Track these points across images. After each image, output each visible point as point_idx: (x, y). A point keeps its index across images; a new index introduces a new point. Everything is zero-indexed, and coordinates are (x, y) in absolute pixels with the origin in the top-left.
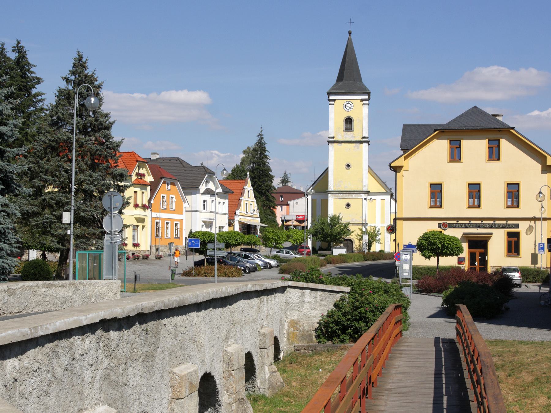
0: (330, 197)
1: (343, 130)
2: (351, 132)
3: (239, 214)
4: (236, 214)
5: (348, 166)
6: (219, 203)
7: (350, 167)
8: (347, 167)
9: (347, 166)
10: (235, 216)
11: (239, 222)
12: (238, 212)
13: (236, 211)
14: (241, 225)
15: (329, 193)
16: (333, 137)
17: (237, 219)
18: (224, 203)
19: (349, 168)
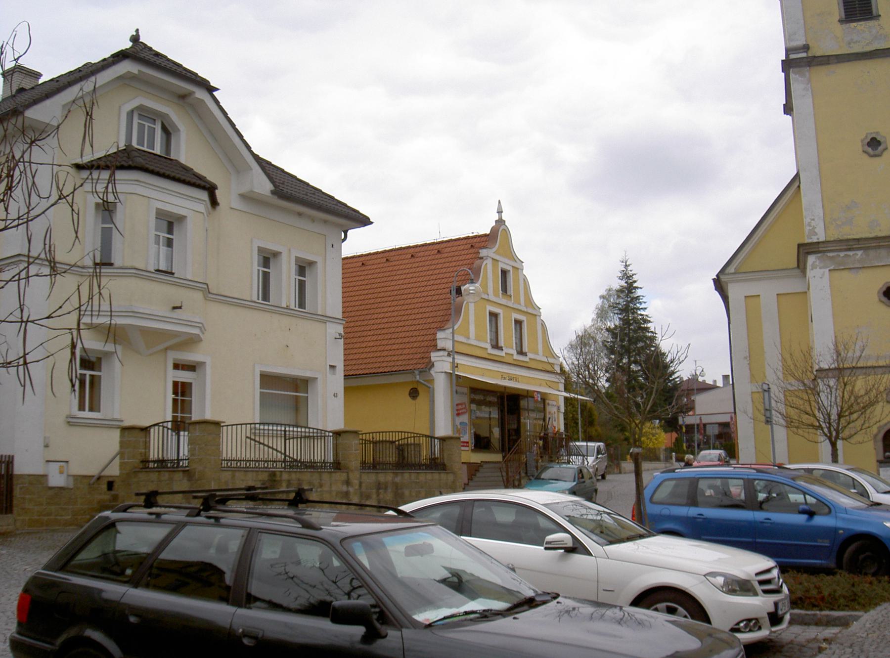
0: (814, 267)
1: (838, 18)
2: (871, 23)
3: (449, 345)
4: (440, 344)
5: (874, 143)
6: (267, 259)
7: (880, 148)
8: (869, 150)
9: (869, 144)
10: (434, 356)
11: (457, 381)
12: (444, 339)
13: (440, 335)
14: (466, 390)
15: (809, 253)
16: (806, 48)
17: (441, 364)
18: (303, 268)
19: (877, 152)
